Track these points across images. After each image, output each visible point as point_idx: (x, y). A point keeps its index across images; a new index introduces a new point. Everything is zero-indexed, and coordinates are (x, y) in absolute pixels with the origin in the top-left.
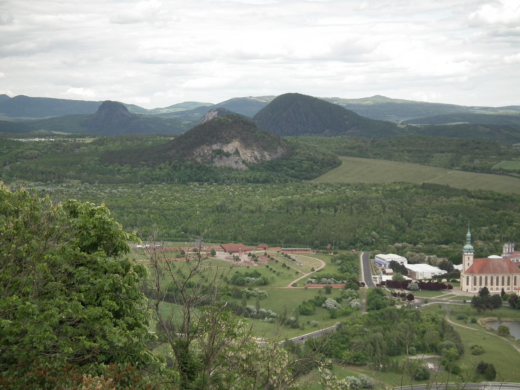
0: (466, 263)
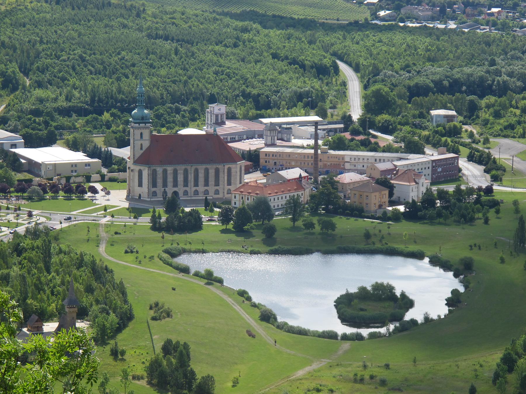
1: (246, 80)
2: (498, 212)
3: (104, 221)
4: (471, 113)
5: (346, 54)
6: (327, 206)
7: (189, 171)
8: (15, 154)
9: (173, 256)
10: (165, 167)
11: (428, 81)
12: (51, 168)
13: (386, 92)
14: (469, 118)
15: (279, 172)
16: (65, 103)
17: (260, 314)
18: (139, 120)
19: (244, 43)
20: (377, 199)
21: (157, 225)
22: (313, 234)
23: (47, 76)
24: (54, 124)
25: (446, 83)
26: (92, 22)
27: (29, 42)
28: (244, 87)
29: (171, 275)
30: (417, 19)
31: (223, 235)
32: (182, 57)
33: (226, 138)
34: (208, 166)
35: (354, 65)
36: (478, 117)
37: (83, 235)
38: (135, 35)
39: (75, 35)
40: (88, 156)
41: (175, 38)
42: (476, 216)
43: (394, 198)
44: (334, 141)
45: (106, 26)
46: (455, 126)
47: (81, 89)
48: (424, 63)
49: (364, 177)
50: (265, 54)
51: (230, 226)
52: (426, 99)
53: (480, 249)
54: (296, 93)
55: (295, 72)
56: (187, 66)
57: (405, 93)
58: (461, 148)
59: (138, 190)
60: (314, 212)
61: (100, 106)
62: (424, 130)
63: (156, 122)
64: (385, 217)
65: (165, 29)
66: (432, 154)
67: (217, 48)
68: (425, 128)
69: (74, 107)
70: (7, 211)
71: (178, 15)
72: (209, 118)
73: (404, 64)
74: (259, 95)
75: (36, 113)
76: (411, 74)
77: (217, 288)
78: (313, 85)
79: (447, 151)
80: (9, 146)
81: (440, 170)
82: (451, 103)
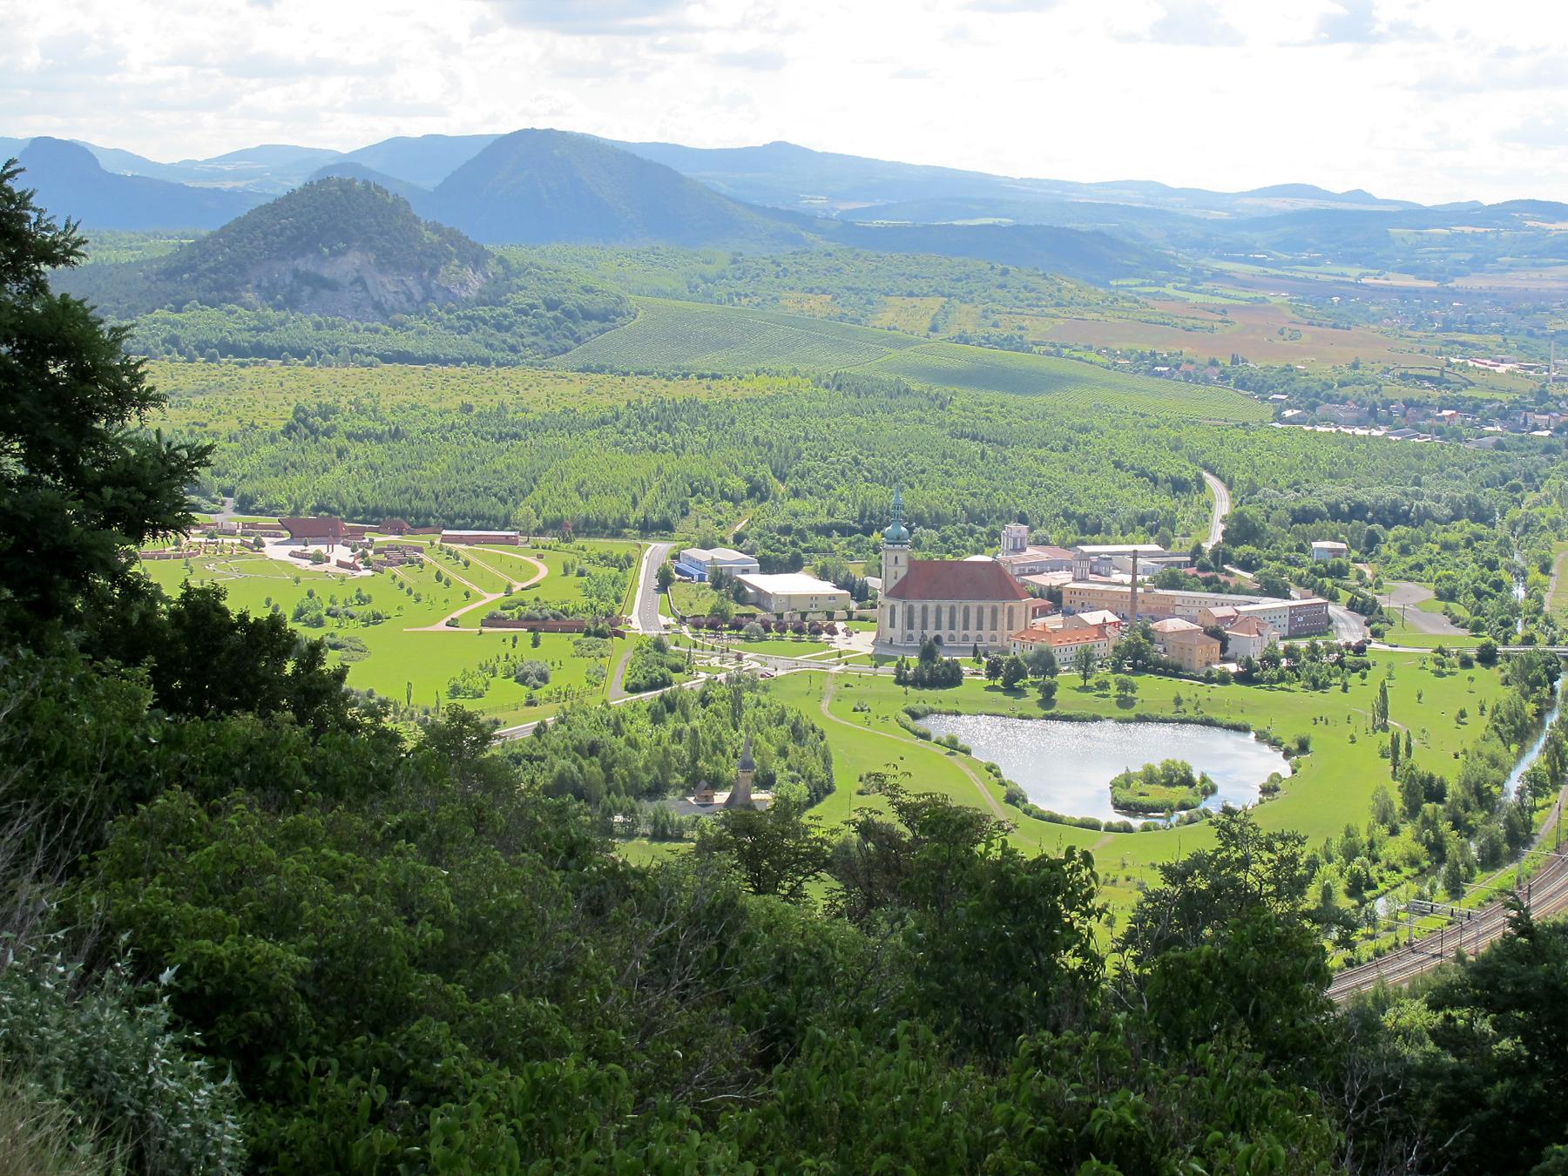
3: (835, 669)
8: (740, 582)
9: (915, 716)
15: (1081, 615)
19: (1078, 444)
23: (809, 482)
25: (1345, 507)
26: (879, 414)
34: (982, 603)
36: (1377, 552)
39: (852, 429)
42: (1334, 681)
48: (1322, 480)
50: (1104, 461)
51: (999, 682)
58: (1340, 591)
59: (889, 633)
60: (1117, 668)
64: (1208, 679)
66: (1298, 598)
67: (1040, 452)
71: (995, 409)
72: (1006, 543)
74: (1086, 516)
75: (786, 530)
81: (1300, 619)
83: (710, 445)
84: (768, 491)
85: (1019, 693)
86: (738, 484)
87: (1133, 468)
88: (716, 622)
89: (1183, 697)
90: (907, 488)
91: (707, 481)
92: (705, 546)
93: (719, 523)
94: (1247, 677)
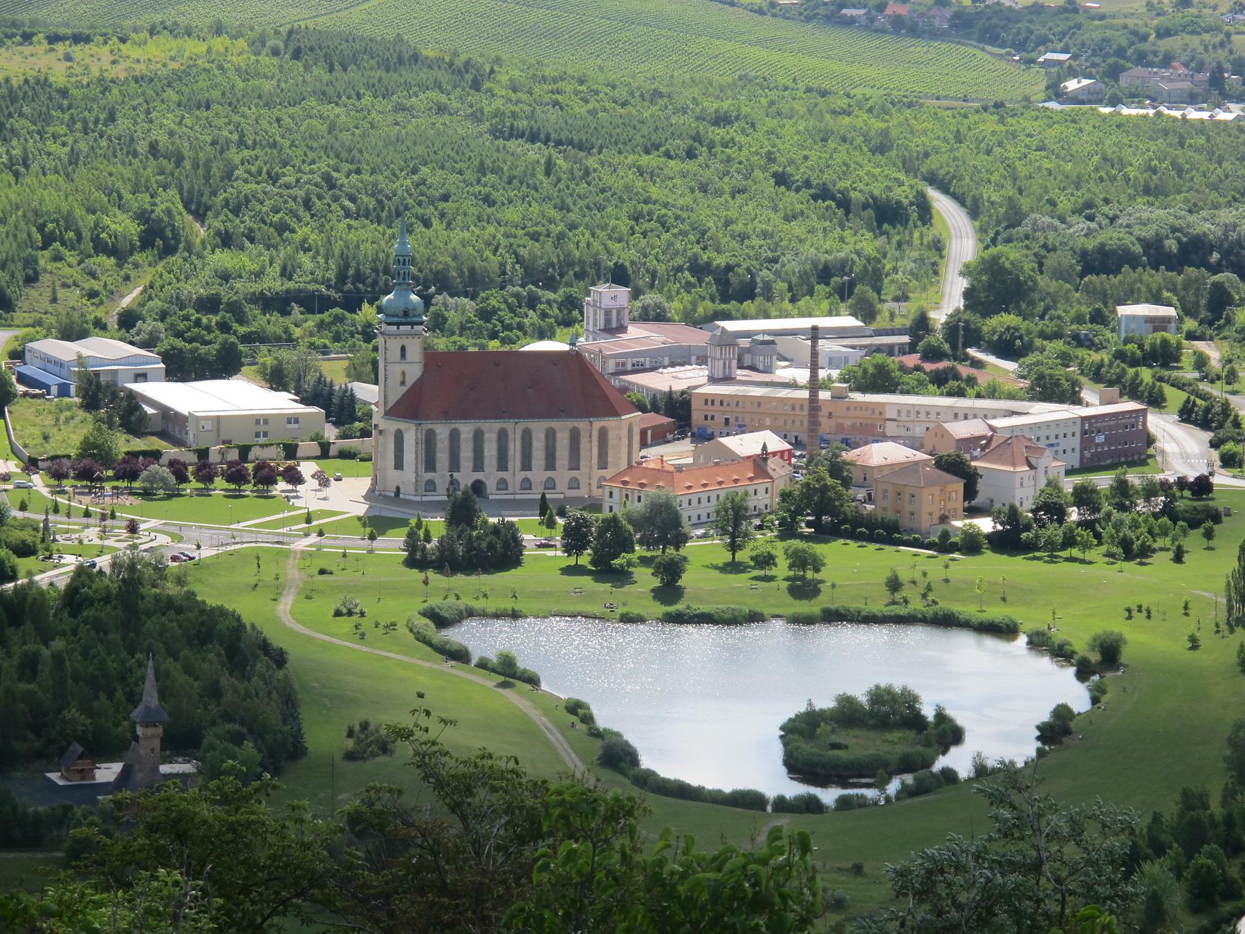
0: (396, 370)
1: (703, 233)
2: (1209, 535)
3: (302, 544)
4: (1215, 311)
5: (954, 177)
6: (819, 518)
7: (511, 435)
8: (132, 395)
9: (442, 622)
10: (453, 426)
11: (1128, 240)
12: (209, 427)
13: (1012, 263)
14: (1211, 324)
15: (721, 440)
16: (279, 283)
17: (600, 752)
18: (398, 316)
19: (711, 146)
20: (938, 500)
21: (418, 556)
22: (770, 579)
23: (248, 221)
24: (242, 330)
25: (1171, 245)
26: (367, 100)
27: (214, 143)
28: (697, 249)
29: (427, 664)
30: (1155, 100)
31: (566, 577)
32: (559, 180)
33: (623, 364)
34: (554, 424)
35: (969, 202)
36: (1229, 321)
37: (247, 575)
38: (465, 128)
40: (305, 401)
41: (554, 136)
42: (1160, 543)
43: (979, 500)
44: (865, 371)
45: (399, 108)
46: (1165, 343)
47: (317, 252)
48: (1132, 198)
49: (921, 456)
50: (758, 174)
51: (585, 559)
52: (1116, 280)
53: (1149, 617)
54: (815, 264)
55: (822, 217)
56: (569, 201)
57: (1071, 266)
58: (1168, 390)
59: (394, 478)
60: (787, 531)
61: (356, 288)
62: (1097, 350)
63: (480, 327)
64: (944, 546)
65: (532, 116)
66: (1095, 403)
67: (645, 160)
68: (1098, 348)
69: (300, 291)
70: (85, 520)
71: (569, 87)
72: (592, 318)
73: (1081, 201)
74: (729, 268)
75: (209, 304)
76: (1093, 225)
77: (521, 694)
78: (858, 247)
79: (1121, 395)
80: (132, 377)
81: (1100, 439)
82: (1174, 290)
83: (74, 158)
84: (176, 236)
85: (620, 577)
86: (123, 225)
87: (807, 184)
88: (89, 468)
89: (904, 576)
90: (419, 228)
91: (69, 221)
92: (71, 333)
93: (92, 294)
94: (1010, 541)
